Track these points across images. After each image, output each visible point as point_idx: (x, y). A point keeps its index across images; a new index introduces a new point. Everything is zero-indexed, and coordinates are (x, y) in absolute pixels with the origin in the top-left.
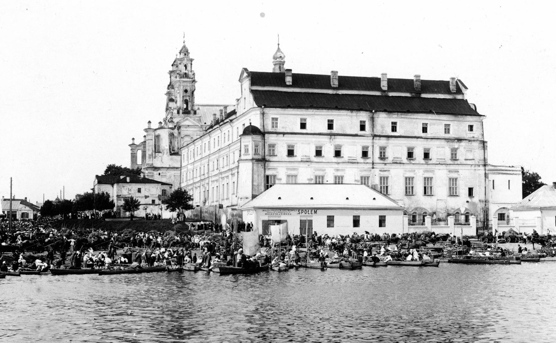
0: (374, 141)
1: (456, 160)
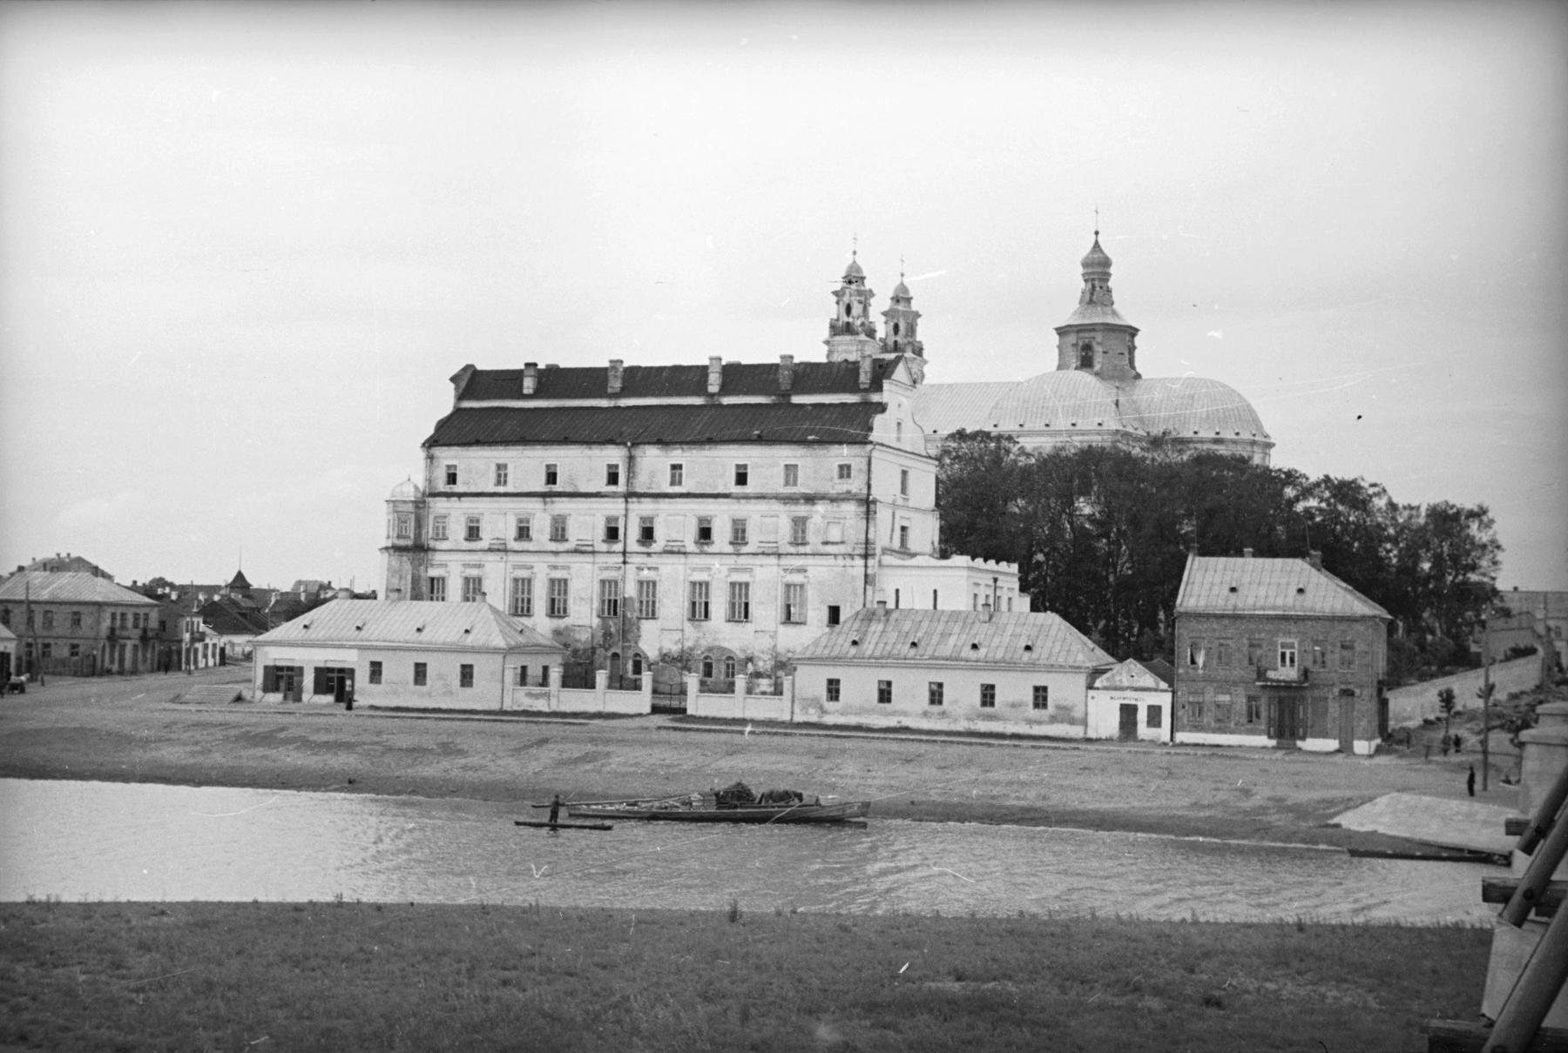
0: (630, 506)
1: (802, 544)
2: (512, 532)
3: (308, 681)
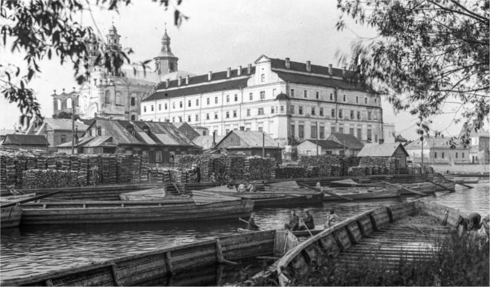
0: (338, 106)
2: (310, 113)
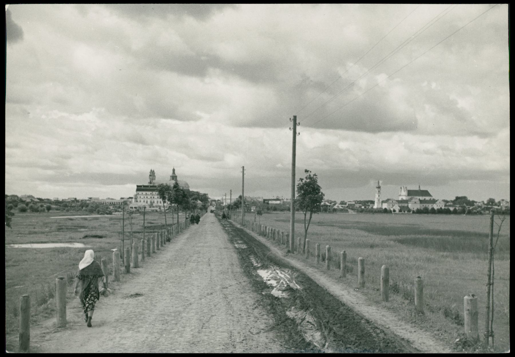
3: (134, 208)
